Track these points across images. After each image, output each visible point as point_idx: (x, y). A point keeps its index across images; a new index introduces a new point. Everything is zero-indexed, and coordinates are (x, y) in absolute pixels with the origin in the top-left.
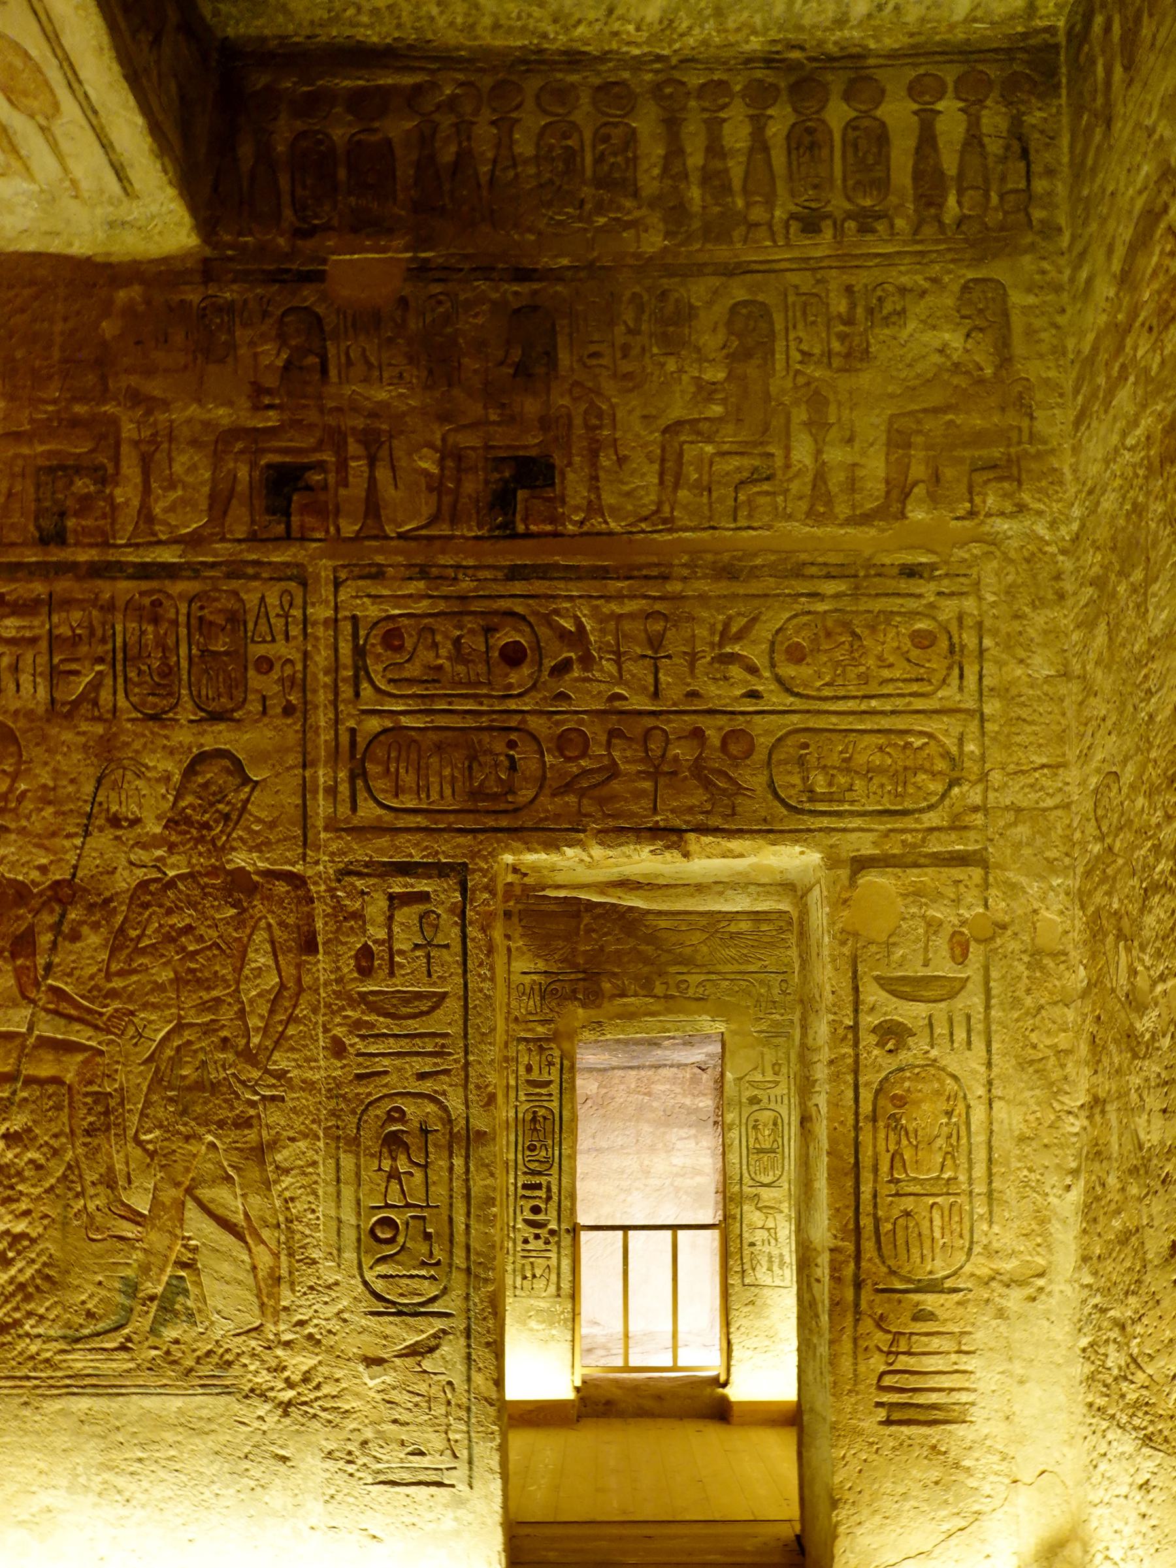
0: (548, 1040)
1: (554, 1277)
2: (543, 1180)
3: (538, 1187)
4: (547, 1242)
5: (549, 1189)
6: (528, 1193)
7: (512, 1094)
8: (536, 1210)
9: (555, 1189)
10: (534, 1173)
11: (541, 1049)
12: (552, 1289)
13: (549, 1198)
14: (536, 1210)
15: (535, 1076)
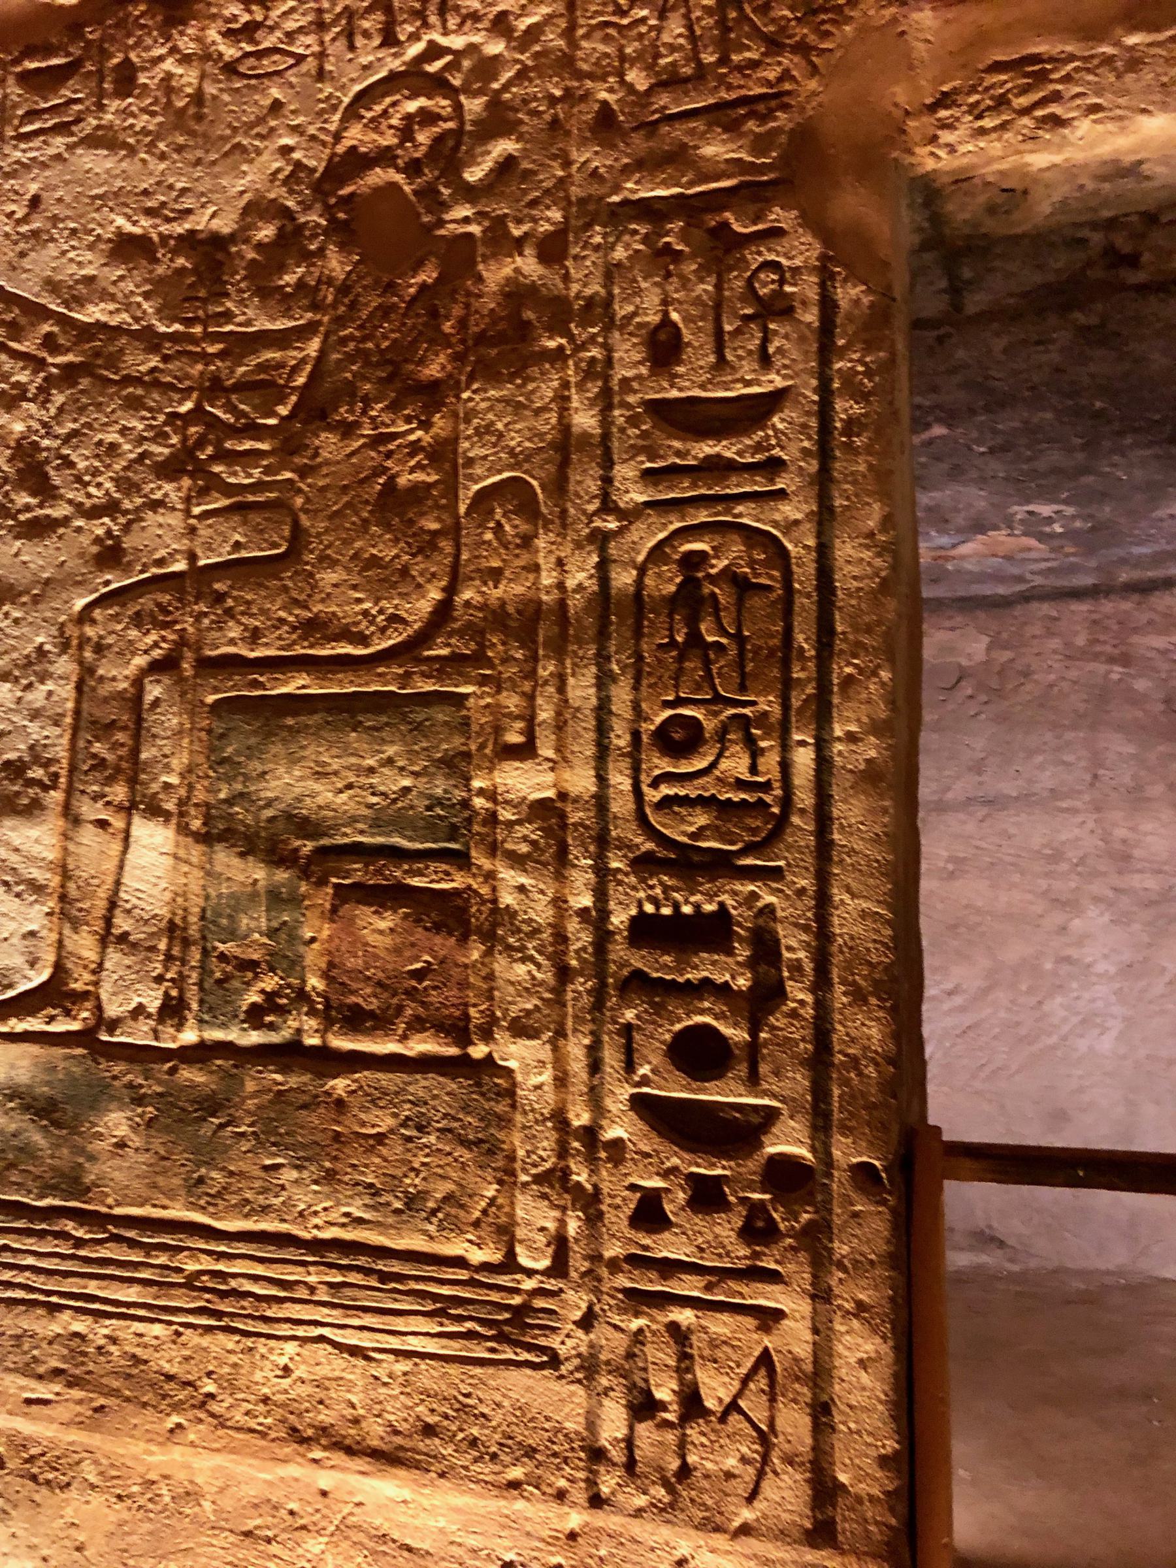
0: (753, 194)
1: (794, 1424)
2: (730, 896)
3: (712, 932)
4: (757, 1231)
5: (765, 949)
6: (659, 965)
7: (585, 482)
8: (699, 1054)
9: (795, 946)
10: (688, 864)
11: (723, 249)
12: (787, 1494)
13: (763, 999)
14: (699, 1054)
15: (689, 384)
